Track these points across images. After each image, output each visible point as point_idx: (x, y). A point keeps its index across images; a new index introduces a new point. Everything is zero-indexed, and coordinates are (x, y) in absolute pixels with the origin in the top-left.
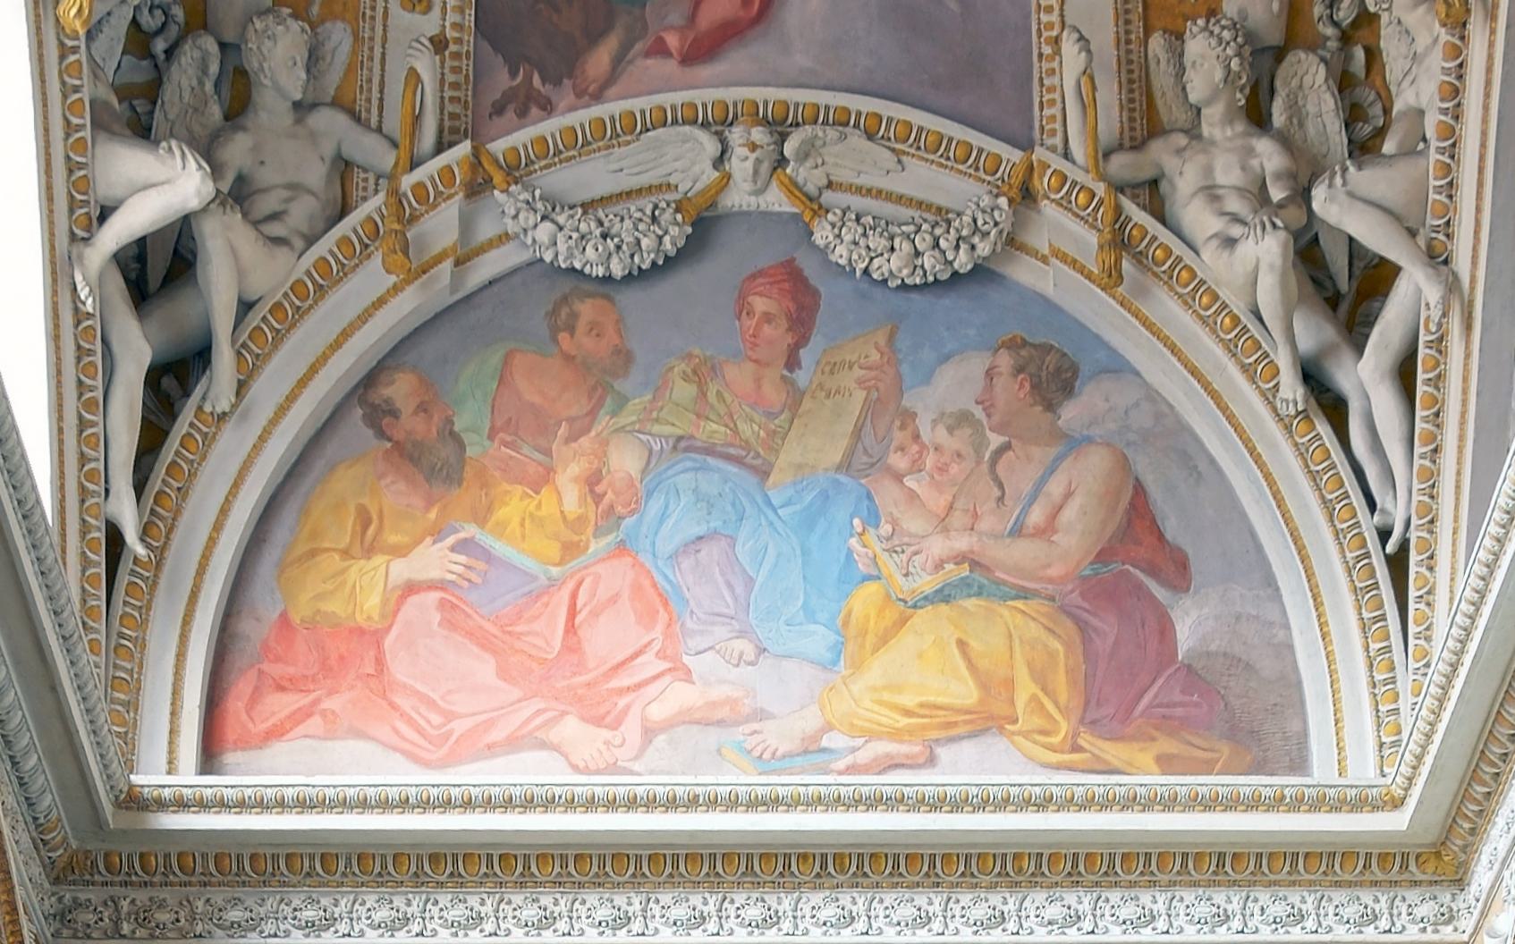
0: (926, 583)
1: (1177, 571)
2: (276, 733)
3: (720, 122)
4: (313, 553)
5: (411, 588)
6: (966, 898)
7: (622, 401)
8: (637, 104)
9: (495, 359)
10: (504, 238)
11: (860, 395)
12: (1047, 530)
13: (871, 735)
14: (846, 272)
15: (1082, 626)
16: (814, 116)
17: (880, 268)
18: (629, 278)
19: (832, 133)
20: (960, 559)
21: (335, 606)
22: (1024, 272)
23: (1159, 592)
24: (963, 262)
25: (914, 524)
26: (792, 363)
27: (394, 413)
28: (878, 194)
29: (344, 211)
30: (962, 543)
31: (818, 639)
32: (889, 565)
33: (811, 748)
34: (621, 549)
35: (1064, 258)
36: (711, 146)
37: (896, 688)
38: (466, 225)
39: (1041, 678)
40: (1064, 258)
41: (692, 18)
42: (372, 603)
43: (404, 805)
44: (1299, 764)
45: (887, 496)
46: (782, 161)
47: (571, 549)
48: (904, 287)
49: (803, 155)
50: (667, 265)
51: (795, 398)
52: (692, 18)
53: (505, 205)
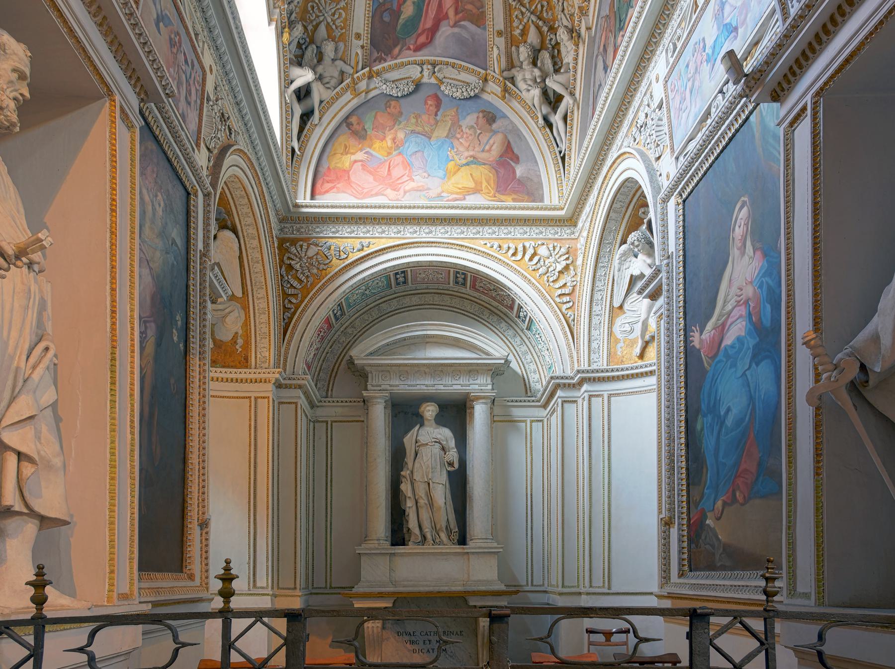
0: (464, 161)
1: (517, 159)
2: (327, 192)
3: (421, 64)
4: (335, 154)
5: (355, 161)
7: (400, 123)
8: (404, 60)
9: (374, 114)
10: (376, 88)
11: (450, 122)
12: (489, 151)
13: (452, 193)
14: (448, 96)
15: (497, 171)
16: (441, 63)
18: (402, 97)
19: (445, 67)
20: (471, 156)
21: (339, 165)
22: (485, 96)
23: (513, 164)
24: (472, 94)
25: (461, 149)
26: (436, 115)
27: (352, 125)
28: (455, 79)
30: (471, 153)
31: (441, 173)
32: (456, 158)
33: (439, 196)
34: (400, 154)
35: (493, 93)
36: (419, 69)
38: (368, 85)
40: (493, 93)
41: (416, 42)
42: (347, 165)
43: (354, 207)
44: (542, 200)
45: (456, 143)
46: (434, 72)
47: (389, 154)
48: (460, 99)
49: (439, 71)
50: (410, 94)
51: (437, 122)
52: (416, 42)
53: (376, 81)
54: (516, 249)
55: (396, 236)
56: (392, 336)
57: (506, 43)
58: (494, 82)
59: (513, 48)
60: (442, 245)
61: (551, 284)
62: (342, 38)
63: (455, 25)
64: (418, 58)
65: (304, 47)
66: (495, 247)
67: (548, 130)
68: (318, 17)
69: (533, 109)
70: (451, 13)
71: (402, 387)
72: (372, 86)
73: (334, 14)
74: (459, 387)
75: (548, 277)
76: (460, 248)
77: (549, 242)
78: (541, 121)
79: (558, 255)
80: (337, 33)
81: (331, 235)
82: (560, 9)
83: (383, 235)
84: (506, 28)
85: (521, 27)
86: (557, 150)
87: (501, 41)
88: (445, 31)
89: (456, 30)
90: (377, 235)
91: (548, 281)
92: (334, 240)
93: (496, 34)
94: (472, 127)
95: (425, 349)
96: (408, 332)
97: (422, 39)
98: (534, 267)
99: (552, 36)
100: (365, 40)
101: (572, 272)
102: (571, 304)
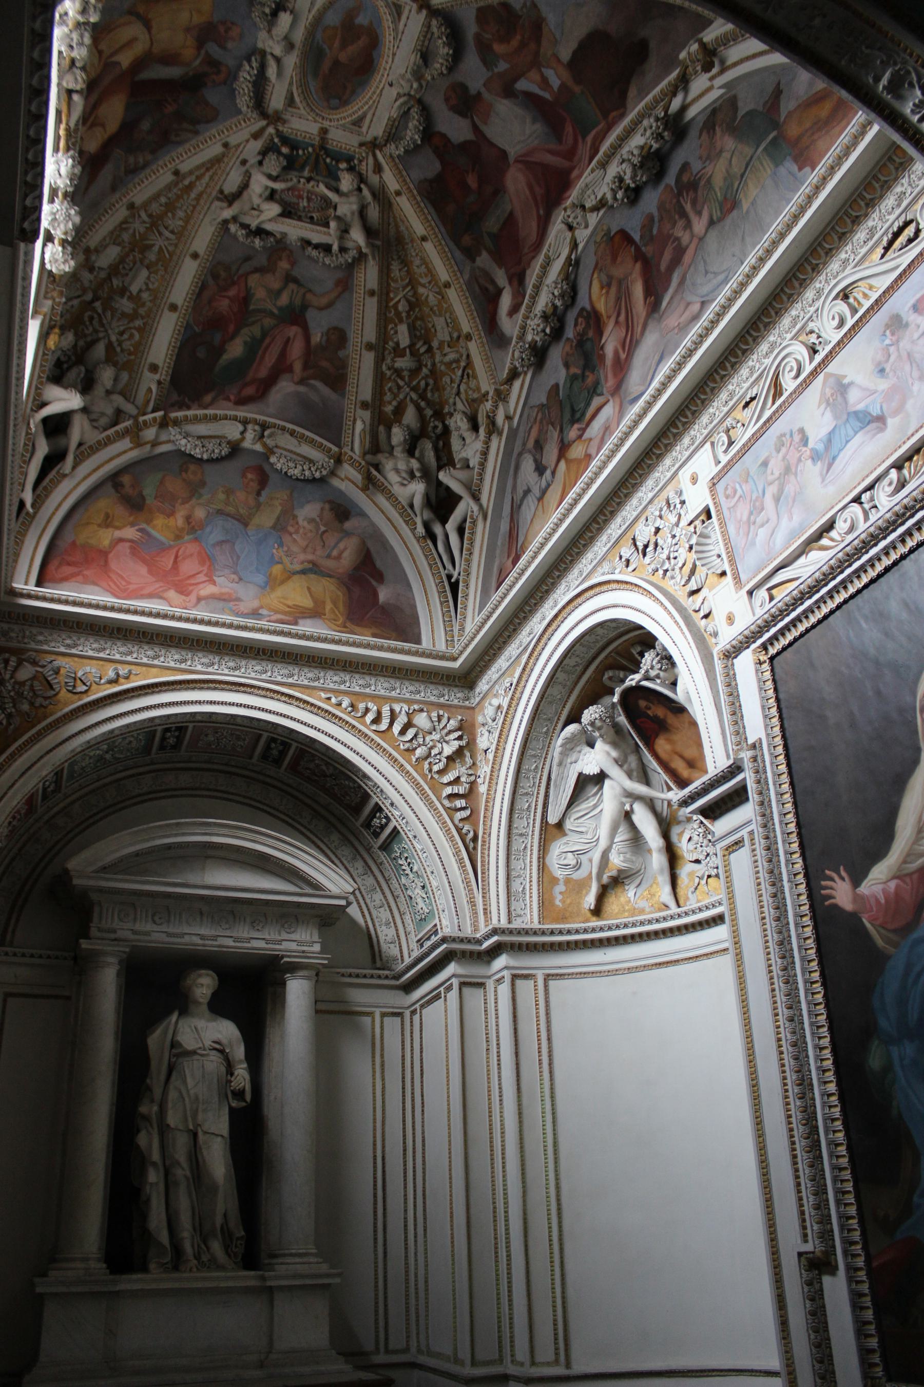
0: (298, 567)
1: (380, 577)
2: (65, 579)
3: (245, 422)
4: (88, 524)
5: (121, 540)
6: (306, 670)
7: (201, 496)
8: (218, 412)
11: (280, 508)
12: (339, 557)
13: (277, 612)
15: (348, 589)
16: (274, 426)
17: (291, 472)
18: (208, 461)
20: (309, 562)
21: (93, 542)
23: (374, 583)
24: (317, 475)
25: (295, 549)
26: (259, 494)
27: (122, 486)
28: (291, 452)
29: (115, 423)
30: (310, 557)
31: (260, 579)
32: (286, 560)
34: (196, 540)
35: (350, 480)
36: (241, 428)
37: (286, 599)
38: (157, 436)
39: (335, 603)
40: (350, 480)
42: (106, 543)
44: (418, 641)
45: (287, 539)
46: (262, 436)
48: (297, 479)
49: (270, 436)
51: (258, 506)
54: (379, 713)
55: (178, 666)
56: (148, 840)
57: (372, 418)
58: (352, 465)
59: (381, 429)
60: (256, 691)
61: (436, 776)
62: (129, 366)
63: (302, 382)
64: (241, 413)
65: (65, 366)
66: (344, 705)
67: (429, 542)
68: (96, 331)
69: (409, 511)
70: (298, 367)
71: (155, 936)
72: (163, 437)
73: (122, 333)
74: (262, 944)
75: (430, 763)
76: (286, 699)
77: (430, 707)
78: (420, 530)
79: (445, 731)
80: (122, 358)
81: (62, 649)
82: (454, 391)
83: (156, 662)
84: (373, 399)
85: (395, 403)
86: (443, 574)
87: (367, 415)
88: (285, 387)
89: (302, 389)
90: (145, 660)
91: (430, 771)
92: (67, 659)
93: (358, 405)
94: (311, 521)
95: (203, 869)
96: (176, 835)
97: (250, 391)
98: (407, 745)
99: (437, 423)
100: (164, 375)
101: (469, 761)
102: (468, 812)
